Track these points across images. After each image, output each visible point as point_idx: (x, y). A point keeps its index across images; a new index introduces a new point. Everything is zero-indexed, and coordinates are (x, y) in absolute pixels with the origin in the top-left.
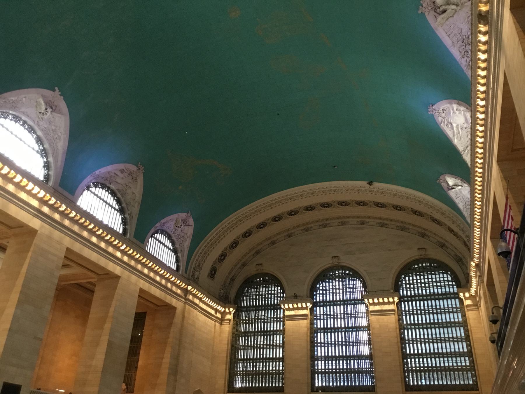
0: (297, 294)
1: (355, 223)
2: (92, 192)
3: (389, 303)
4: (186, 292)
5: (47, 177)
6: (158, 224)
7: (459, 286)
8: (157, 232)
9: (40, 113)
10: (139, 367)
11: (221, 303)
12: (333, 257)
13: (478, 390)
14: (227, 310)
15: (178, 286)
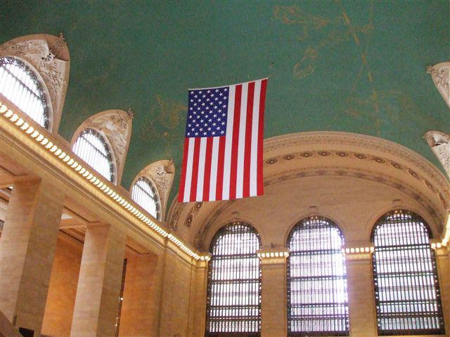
0: (274, 243)
1: (333, 173)
2: (84, 139)
3: (365, 253)
4: (167, 239)
5: (47, 124)
6: (142, 172)
7: (431, 237)
8: (140, 179)
9: (43, 58)
10: (122, 312)
11: (197, 251)
12: (311, 207)
13: (445, 334)
14: (202, 258)
15: (160, 235)
